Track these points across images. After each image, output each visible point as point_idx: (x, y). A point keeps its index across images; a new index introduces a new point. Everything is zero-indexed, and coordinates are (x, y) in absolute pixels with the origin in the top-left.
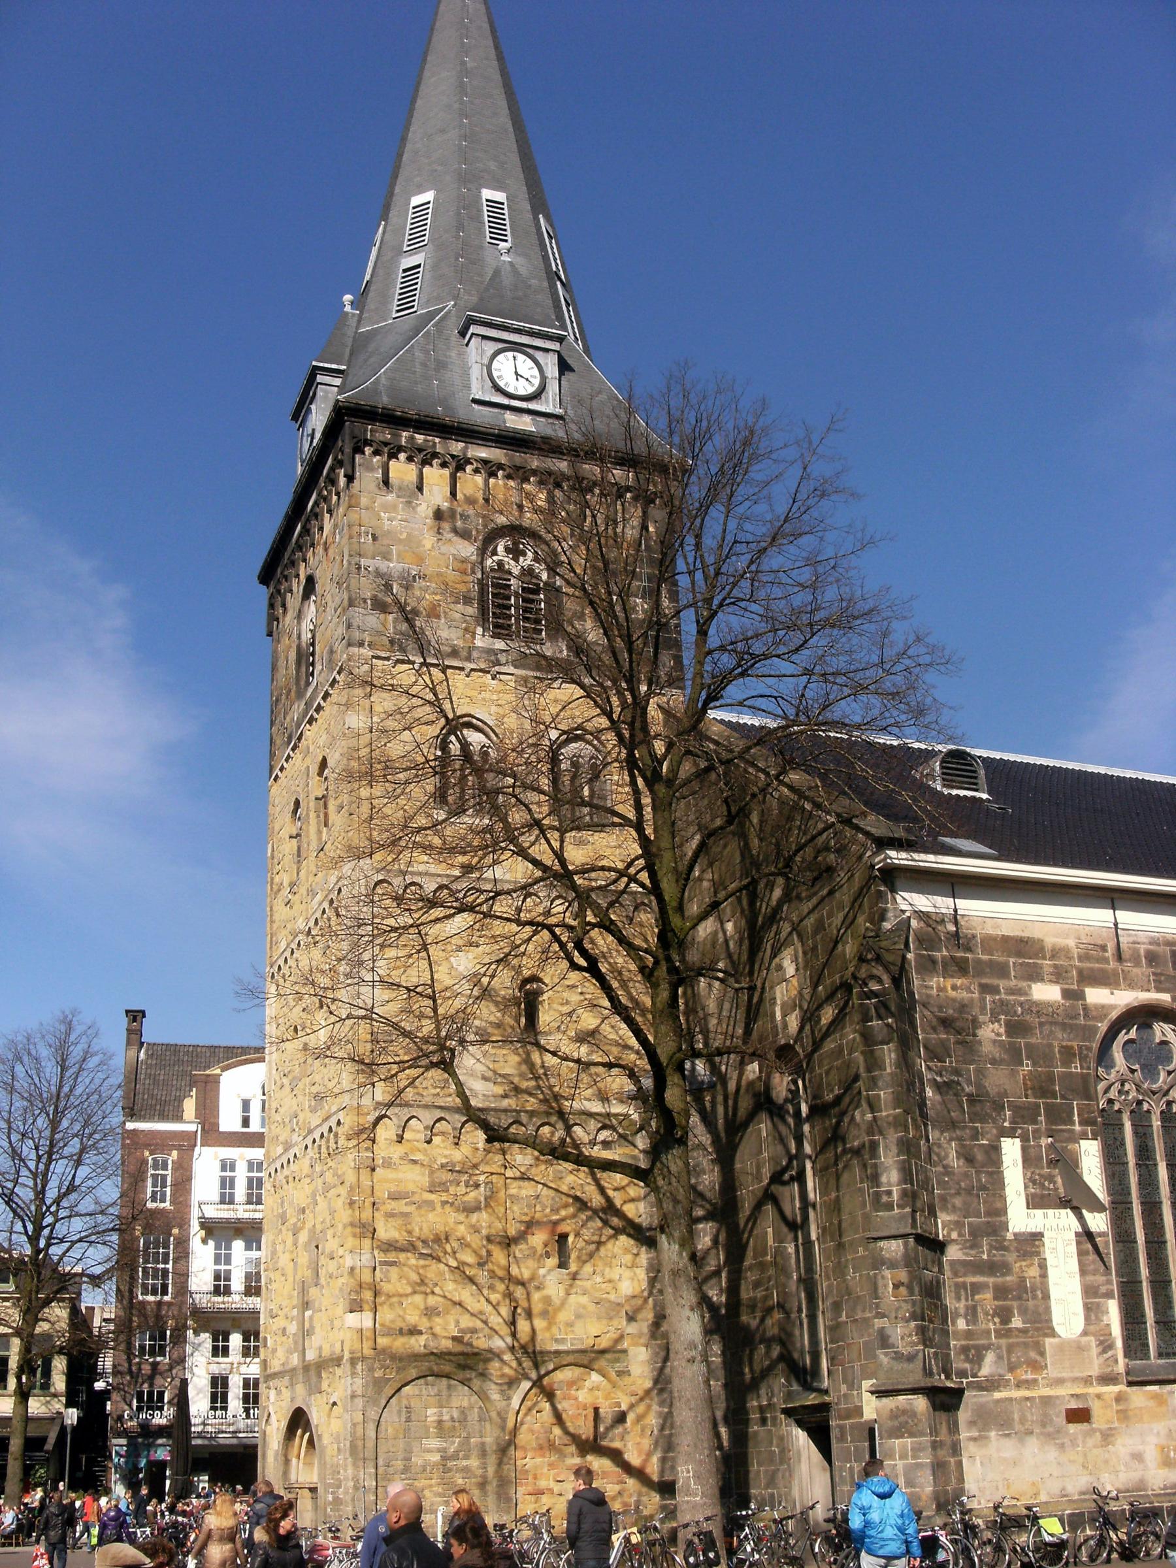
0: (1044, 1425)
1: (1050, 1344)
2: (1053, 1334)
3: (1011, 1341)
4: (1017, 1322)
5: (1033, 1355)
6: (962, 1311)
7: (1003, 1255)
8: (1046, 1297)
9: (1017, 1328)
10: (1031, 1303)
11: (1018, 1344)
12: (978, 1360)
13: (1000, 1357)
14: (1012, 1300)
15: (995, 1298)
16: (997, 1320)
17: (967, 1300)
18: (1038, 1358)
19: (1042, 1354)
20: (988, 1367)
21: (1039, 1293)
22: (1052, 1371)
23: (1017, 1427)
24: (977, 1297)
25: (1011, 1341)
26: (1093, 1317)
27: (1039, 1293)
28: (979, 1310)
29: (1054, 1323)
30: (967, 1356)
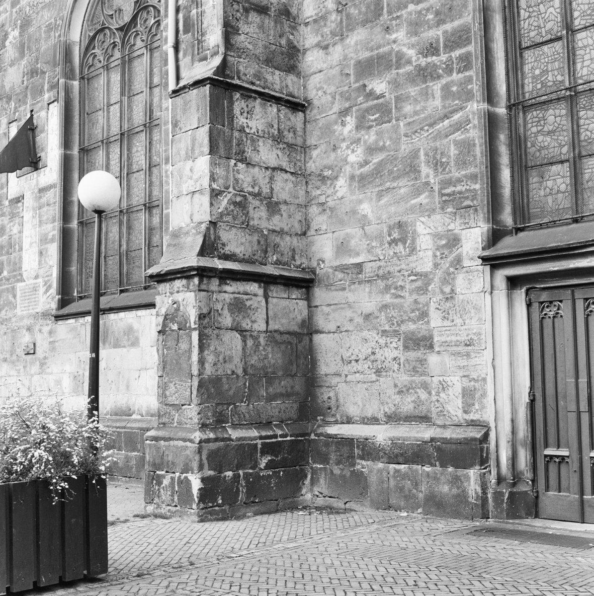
8: (21, 249)
19: (15, 296)
22: (18, 311)
29: (23, 270)
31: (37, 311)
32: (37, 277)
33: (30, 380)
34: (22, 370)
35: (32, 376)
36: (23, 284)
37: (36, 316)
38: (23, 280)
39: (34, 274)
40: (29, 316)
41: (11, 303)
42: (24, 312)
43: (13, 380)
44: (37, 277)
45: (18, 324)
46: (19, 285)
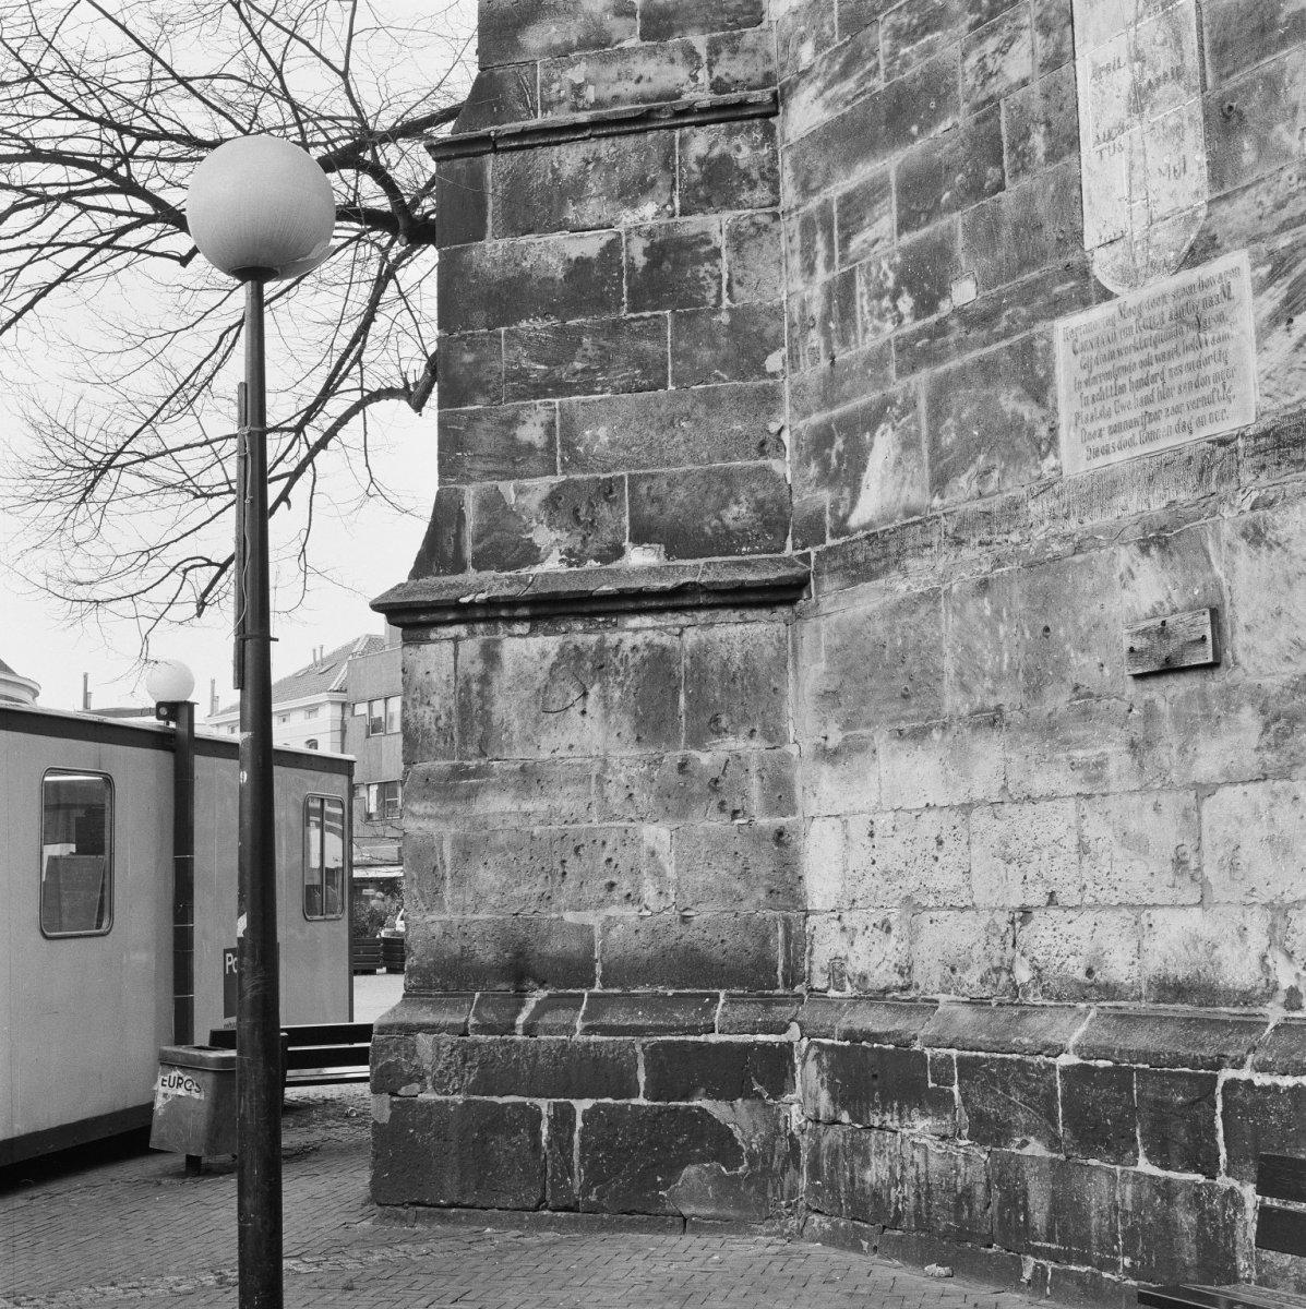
0: (1034, 690)
1: (1071, 335)
2: (1088, 292)
3: (941, 369)
4: (964, 292)
5: (1010, 402)
6: (816, 309)
7: (930, 49)
8: (1066, 141)
9: (959, 312)
10: (1007, 197)
11: (962, 375)
12: (848, 474)
13: (908, 443)
14: (949, 209)
15: (904, 225)
16: (906, 303)
17: (829, 264)
18: (1028, 411)
19: (1039, 391)
20: (883, 488)
21: (1038, 142)
22: (1072, 459)
23: (953, 701)
24: (856, 244)
25: (941, 369)
26: (1248, 157)
27: (1038, 142)
28: (860, 287)
29: (1090, 241)
30: (825, 464)
31: (1222, 429)
32: (1202, 250)
33: (1190, 818)
34: (1118, 760)
35: (1204, 790)
36: (1099, 313)
37: (1213, 462)
38: (1088, 292)
39: (1172, 239)
40: (1156, 471)
41: (1016, 426)
42: (1117, 457)
43: (1057, 823)
44: (1202, 250)
45: (1072, 525)
46: (1067, 333)
